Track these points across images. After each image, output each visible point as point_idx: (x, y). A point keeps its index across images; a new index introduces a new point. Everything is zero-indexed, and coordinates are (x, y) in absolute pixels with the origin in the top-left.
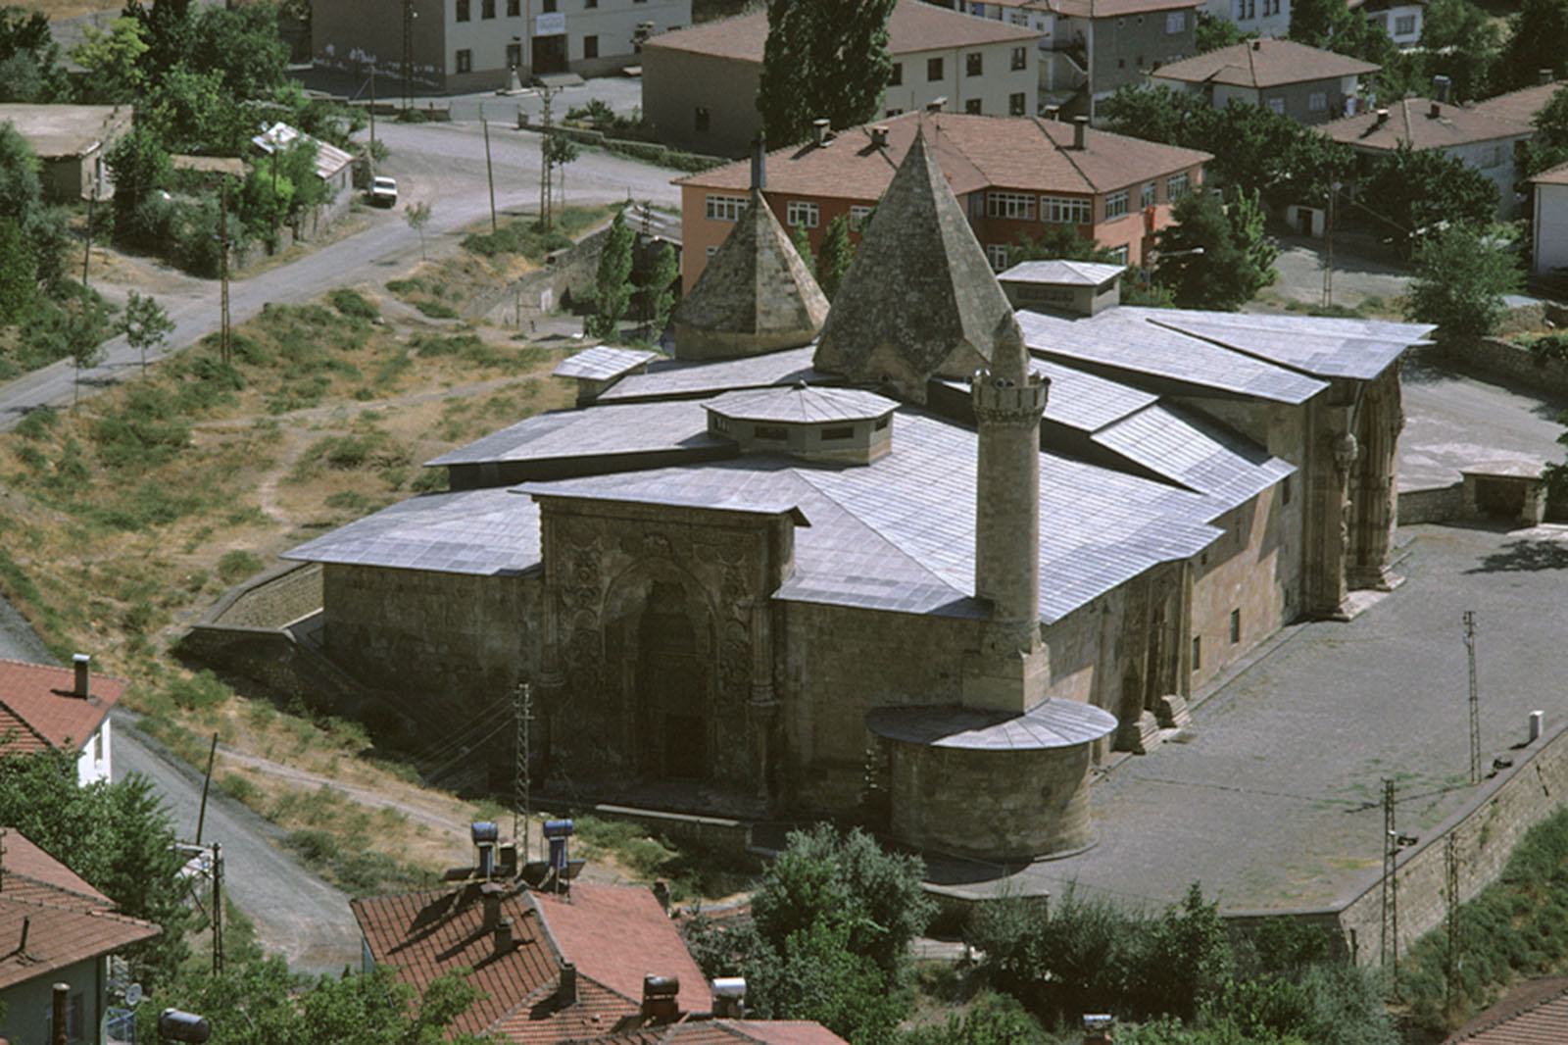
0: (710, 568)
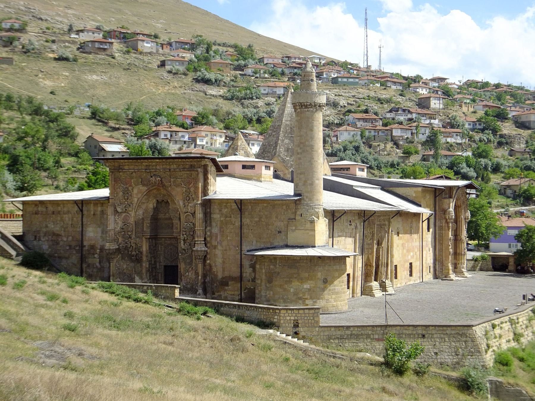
0: (179, 189)
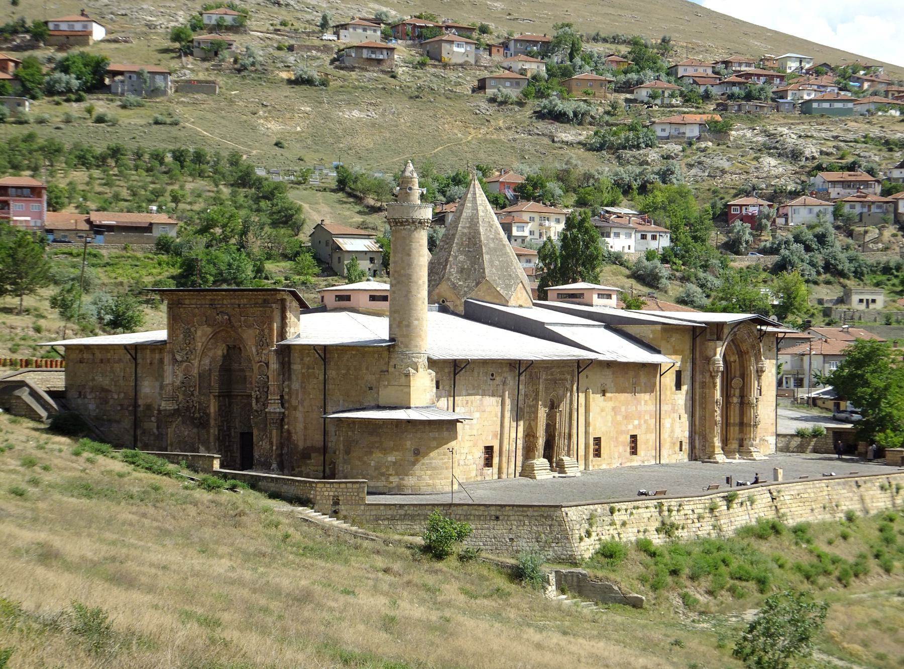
0: (250, 331)
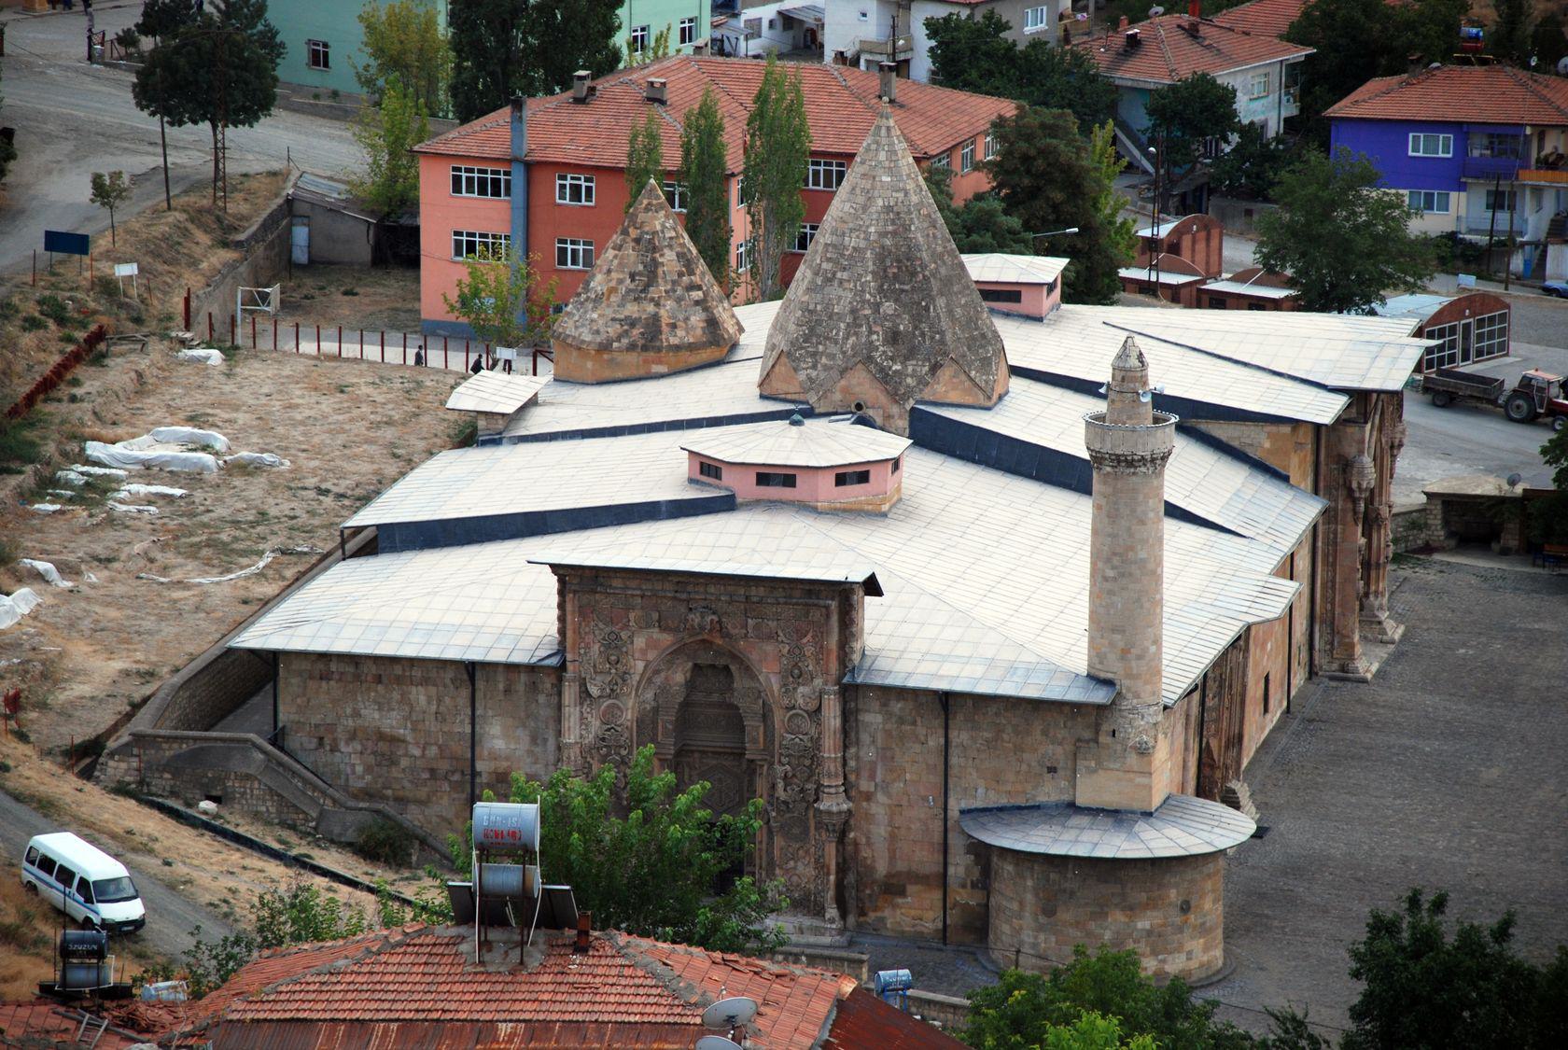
0: (769, 648)
